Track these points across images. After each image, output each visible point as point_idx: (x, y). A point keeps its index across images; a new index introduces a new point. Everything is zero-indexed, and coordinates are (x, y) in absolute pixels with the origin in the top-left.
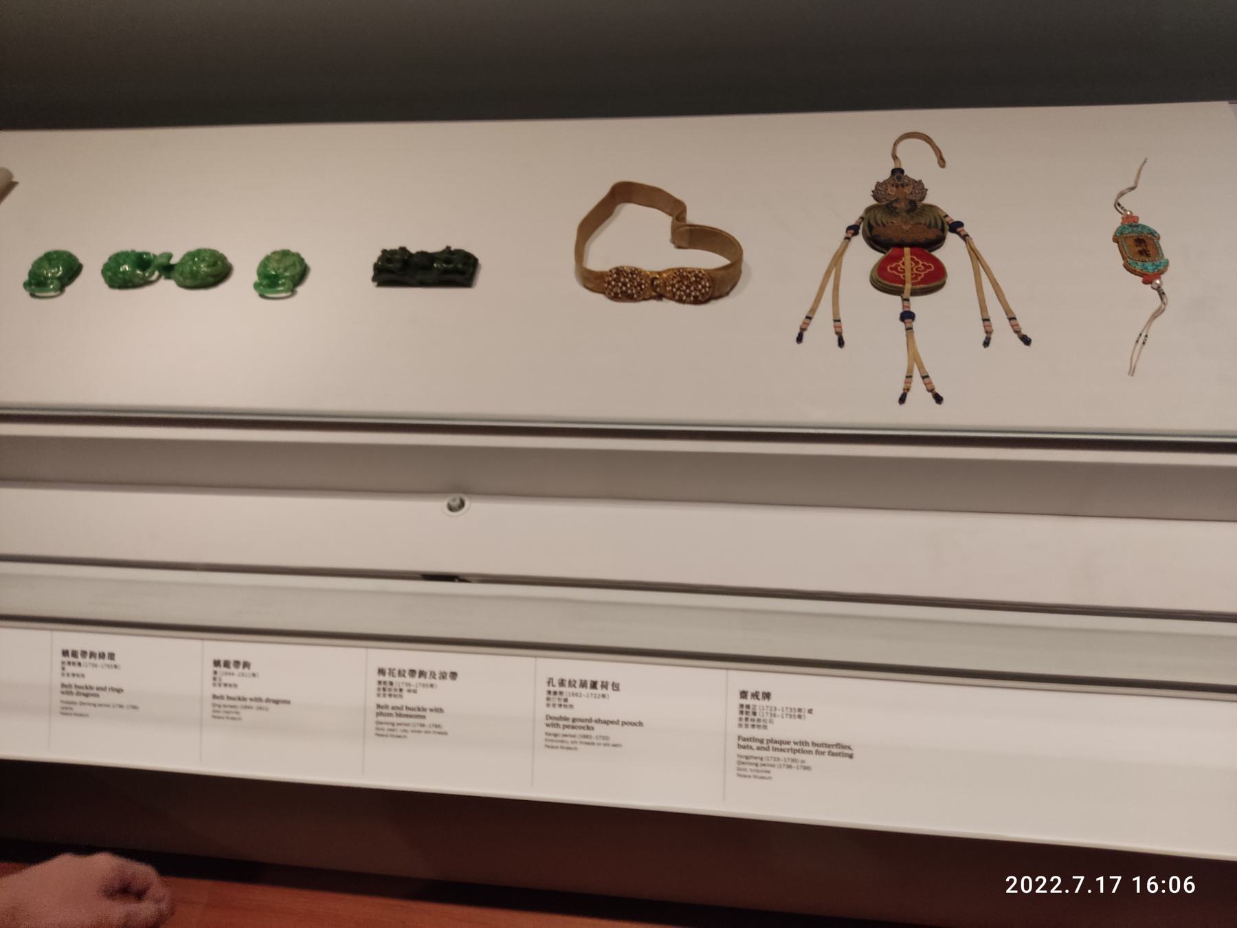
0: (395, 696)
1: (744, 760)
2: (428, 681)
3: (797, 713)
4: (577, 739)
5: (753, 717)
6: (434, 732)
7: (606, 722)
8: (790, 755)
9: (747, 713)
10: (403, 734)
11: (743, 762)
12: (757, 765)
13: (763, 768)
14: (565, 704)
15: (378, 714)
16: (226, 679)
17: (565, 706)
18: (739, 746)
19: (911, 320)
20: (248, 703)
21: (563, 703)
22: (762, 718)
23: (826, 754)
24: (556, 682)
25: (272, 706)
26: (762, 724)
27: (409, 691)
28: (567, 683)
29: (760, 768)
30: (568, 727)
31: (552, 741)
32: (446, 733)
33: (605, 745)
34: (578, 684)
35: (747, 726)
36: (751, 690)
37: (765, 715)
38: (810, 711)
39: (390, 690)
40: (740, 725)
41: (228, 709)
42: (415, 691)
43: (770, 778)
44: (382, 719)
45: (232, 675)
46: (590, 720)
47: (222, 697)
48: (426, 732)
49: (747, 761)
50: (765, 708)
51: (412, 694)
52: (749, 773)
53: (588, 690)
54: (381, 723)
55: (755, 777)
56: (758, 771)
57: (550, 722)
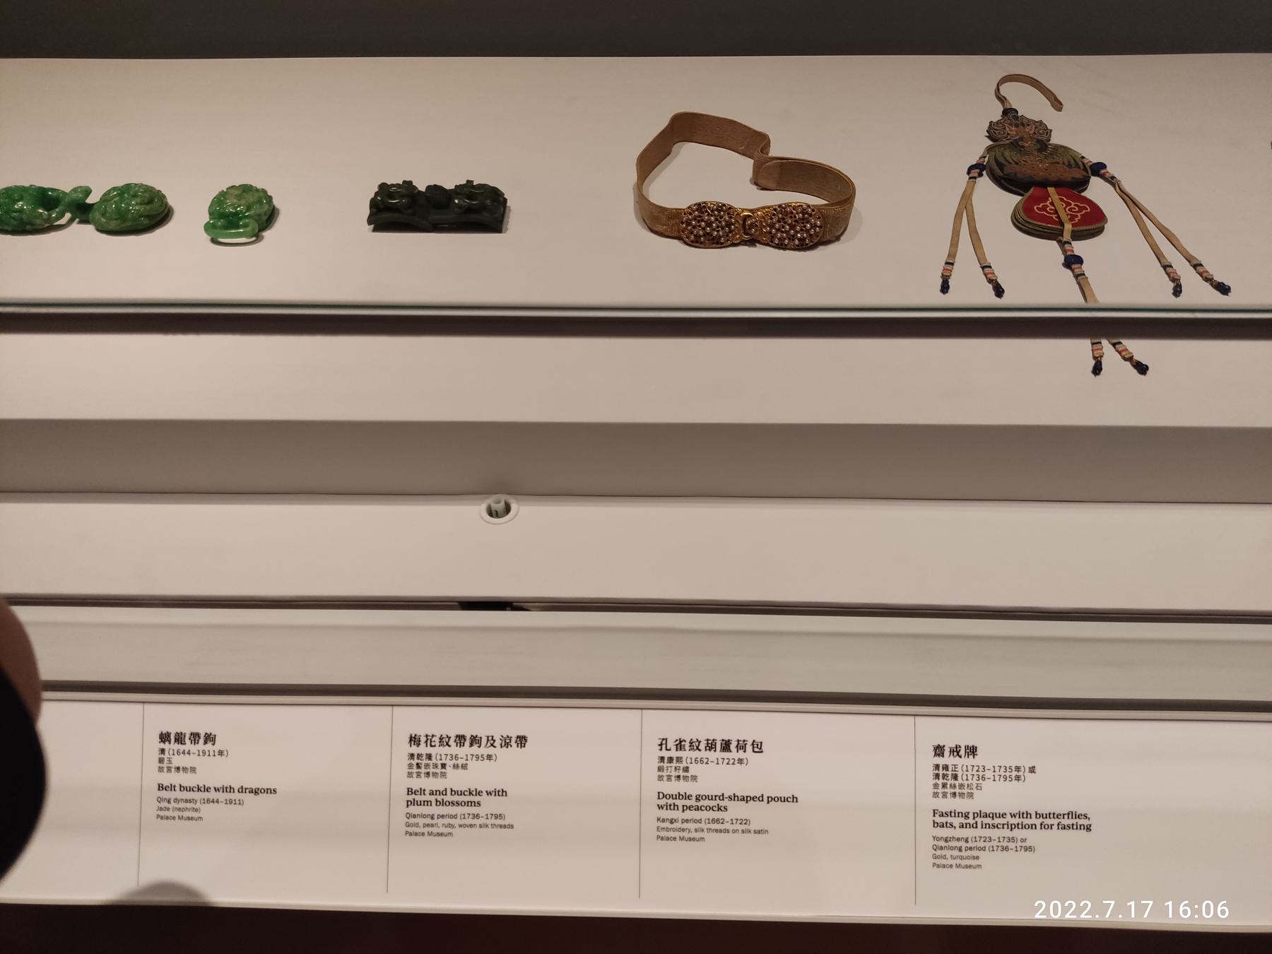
0: (435, 774)
1: (942, 843)
2: (484, 751)
3: (1014, 774)
4: (703, 825)
5: (953, 782)
6: (493, 825)
7: (746, 799)
8: (1006, 833)
9: (944, 776)
10: (449, 830)
11: (940, 846)
12: (960, 850)
13: (969, 853)
14: (685, 775)
15: (409, 803)
16: (178, 761)
17: (685, 778)
18: (935, 824)
19: (1079, 265)
20: (212, 795)
21: (681, 773)
22: (966, 783)
23: (1055, 827)
24: (671, 744)
25: (248, 797)
26: (966, 791)
27: (456, 766)
28: (687, 745)
29: (964, 853)
30: (689, 808)
31: (668, 830)
32: (512, 827)
33: (743, 832)
34: (702, 746)
35: (945, 795)
36: (949, 744)
37: (970, 777)
38: (1032, 770)
39: (427, 766)
40: (936, 795)
41: (182, 805)
42: (464, 767)
43: (979, 866)
44: (414, 810)
45: (191, 756)
46: (722, 797)
47: (172, 788)
48: (481, 826)
49: (946, 844)
50: (970, 768)
51: (460, 771)
52: (950, 862)
53: (718, 754)
54: (414, 816)
55: (958, 866)
56: (962, 858)
57: (663, 802)
